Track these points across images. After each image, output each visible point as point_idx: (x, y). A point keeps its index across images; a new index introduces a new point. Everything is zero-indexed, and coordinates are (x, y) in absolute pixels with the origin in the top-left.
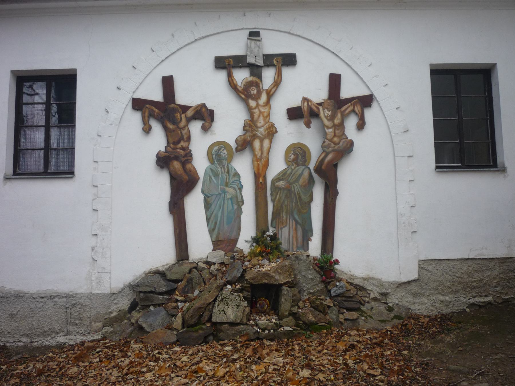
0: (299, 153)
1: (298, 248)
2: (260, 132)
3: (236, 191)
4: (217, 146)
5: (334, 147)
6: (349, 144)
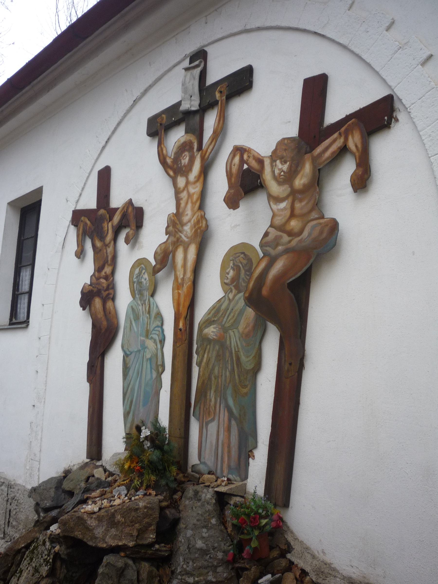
0: (241, 263)
1: (229, 467)
2: (185, 233)
3: (156, 345)
4: (138, 266)
5: (290, 241)
6: (326, 230)
